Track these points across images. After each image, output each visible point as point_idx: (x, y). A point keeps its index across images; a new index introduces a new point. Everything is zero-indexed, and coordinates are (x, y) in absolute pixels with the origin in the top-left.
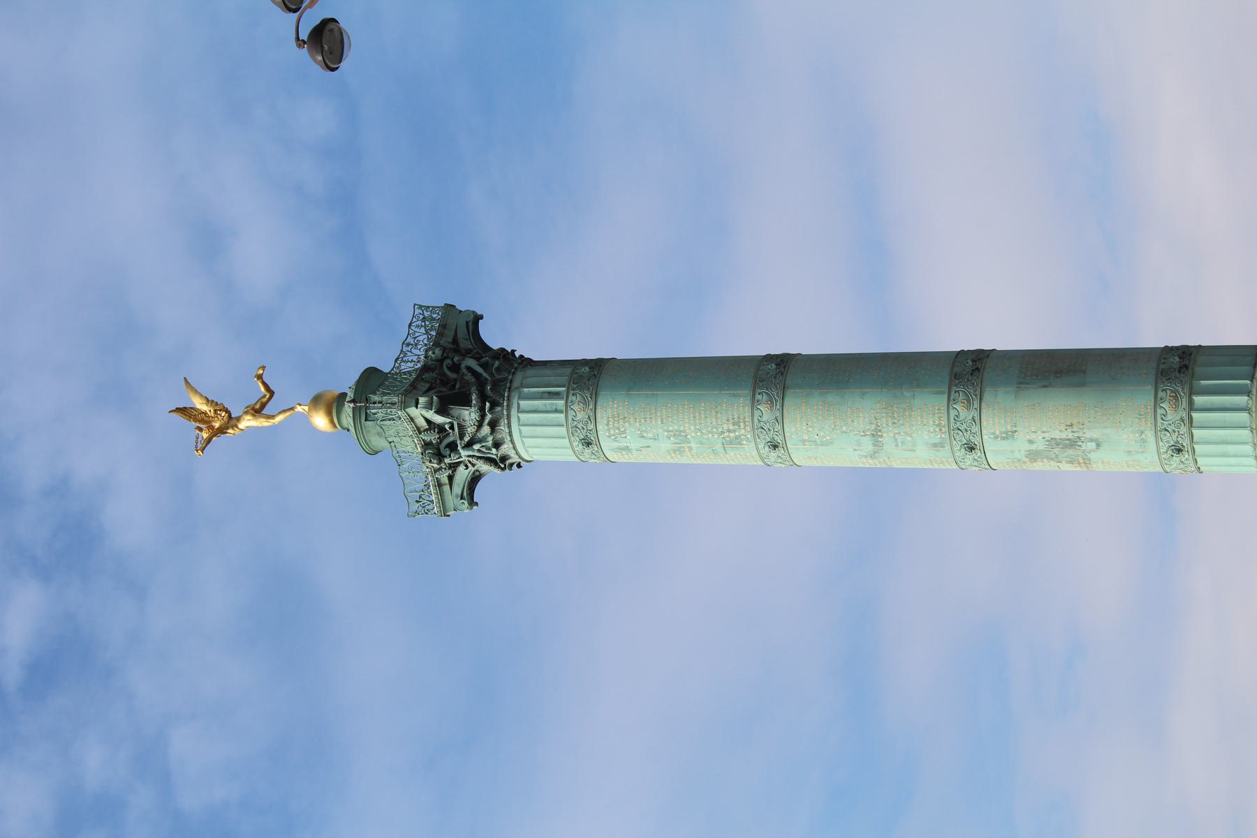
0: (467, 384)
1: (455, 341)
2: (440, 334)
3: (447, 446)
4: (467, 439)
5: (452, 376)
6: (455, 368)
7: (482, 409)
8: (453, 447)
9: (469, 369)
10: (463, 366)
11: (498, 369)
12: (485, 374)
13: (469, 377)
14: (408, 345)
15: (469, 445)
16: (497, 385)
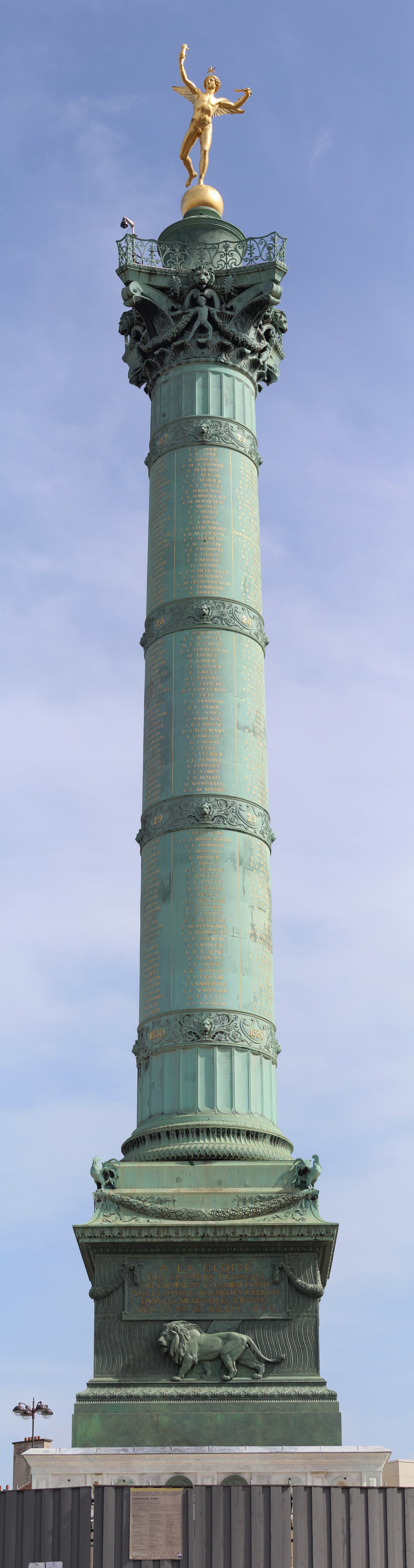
0: (177, 318)
1: (241, 290)
2: (239, 272)
3: (137, 332)
4: (142, 347)
5: (187, 302)
6: (194, 303)
7: (156, 348)
8: (137, 337)
9: (195, 317)
10: (197, 308)
11: (202, 346)
12: (192, 334)
13: (186, 319)
14: (226, 248)
15: (140, 351)
16: (182, 347)
